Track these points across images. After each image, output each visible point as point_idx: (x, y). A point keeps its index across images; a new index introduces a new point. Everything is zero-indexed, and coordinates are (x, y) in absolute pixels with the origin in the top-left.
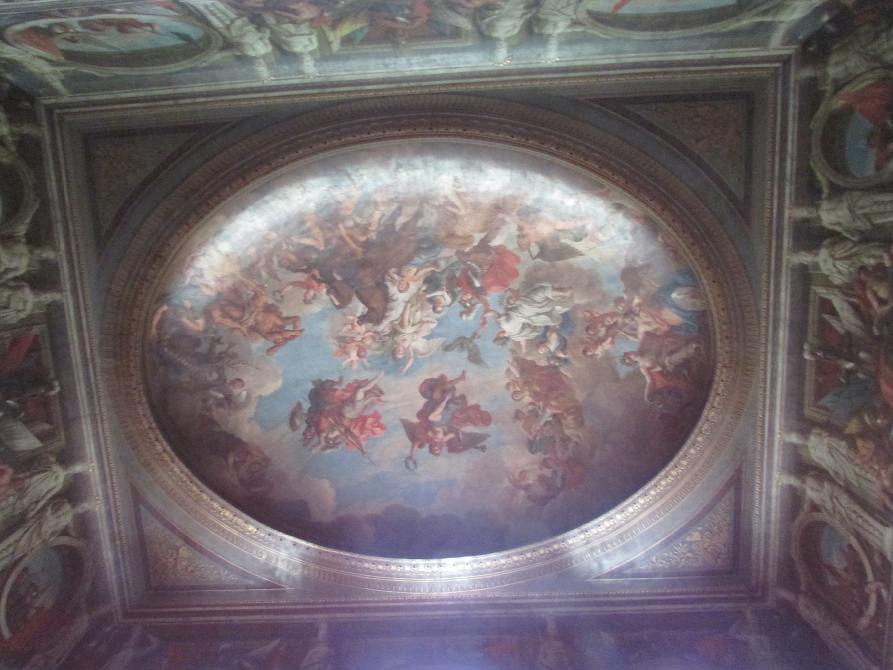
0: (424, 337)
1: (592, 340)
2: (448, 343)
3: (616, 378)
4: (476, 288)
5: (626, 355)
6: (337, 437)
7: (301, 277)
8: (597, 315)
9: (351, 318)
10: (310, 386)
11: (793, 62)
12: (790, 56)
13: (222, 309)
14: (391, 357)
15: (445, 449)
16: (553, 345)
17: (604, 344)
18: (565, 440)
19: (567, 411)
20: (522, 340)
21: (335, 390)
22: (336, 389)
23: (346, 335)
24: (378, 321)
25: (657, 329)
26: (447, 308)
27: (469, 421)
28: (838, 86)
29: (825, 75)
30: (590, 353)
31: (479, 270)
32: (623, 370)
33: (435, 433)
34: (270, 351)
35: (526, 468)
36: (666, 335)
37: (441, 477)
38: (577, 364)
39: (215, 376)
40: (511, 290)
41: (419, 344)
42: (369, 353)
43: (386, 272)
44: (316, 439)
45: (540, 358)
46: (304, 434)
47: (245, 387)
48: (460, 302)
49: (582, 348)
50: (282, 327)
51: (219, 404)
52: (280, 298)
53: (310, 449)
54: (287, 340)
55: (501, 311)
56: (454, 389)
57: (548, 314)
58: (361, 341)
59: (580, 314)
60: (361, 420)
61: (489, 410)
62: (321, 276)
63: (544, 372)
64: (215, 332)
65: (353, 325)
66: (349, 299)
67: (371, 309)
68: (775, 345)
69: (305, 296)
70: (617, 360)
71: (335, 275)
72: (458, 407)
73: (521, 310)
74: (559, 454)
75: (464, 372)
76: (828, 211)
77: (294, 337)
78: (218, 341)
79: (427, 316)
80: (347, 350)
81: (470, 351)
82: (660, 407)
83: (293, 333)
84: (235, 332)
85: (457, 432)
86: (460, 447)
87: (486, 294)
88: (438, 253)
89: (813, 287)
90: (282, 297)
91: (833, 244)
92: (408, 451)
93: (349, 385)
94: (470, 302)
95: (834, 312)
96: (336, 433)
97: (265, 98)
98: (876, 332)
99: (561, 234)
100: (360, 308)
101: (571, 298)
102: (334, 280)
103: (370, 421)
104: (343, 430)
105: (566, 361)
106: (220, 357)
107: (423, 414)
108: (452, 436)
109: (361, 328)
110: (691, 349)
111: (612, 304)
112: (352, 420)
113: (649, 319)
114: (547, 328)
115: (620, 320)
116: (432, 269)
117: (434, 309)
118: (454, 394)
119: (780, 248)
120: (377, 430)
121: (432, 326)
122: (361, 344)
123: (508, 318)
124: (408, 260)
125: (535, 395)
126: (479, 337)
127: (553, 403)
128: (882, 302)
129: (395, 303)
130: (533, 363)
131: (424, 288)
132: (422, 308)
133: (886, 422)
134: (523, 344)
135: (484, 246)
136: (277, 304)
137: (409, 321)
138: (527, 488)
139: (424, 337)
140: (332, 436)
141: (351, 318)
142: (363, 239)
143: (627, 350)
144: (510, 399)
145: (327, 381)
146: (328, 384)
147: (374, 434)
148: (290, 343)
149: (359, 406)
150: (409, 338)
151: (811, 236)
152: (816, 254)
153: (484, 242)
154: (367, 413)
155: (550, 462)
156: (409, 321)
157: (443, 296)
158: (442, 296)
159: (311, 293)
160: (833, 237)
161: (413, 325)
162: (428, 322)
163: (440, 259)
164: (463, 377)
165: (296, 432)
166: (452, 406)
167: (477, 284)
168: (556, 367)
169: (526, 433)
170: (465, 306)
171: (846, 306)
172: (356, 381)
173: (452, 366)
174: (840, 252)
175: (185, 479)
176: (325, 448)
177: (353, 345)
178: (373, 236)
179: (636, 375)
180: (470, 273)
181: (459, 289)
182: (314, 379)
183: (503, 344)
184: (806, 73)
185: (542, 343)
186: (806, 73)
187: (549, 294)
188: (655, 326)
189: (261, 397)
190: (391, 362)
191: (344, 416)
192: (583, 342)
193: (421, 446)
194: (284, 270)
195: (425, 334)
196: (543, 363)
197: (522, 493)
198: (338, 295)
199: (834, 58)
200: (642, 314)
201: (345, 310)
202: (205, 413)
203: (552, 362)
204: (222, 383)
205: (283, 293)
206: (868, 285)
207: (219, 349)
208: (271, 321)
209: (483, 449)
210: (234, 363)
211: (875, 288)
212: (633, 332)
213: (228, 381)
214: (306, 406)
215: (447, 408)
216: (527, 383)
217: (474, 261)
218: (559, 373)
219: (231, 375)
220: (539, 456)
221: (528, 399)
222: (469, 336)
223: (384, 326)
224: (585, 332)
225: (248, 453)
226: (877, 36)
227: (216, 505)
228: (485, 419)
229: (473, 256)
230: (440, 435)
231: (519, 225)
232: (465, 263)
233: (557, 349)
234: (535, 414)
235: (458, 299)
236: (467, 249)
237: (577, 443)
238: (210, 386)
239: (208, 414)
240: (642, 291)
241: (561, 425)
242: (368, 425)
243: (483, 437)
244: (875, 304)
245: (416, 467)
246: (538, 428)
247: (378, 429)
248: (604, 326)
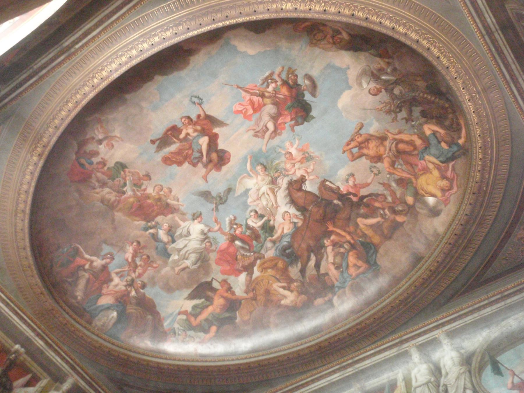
0: (250, 190)
1: (140, 252)
2: (231, 193)
3: (105, 242)
4: (237, 240)
5: (113, 259)
6: (268, 87)
7: (363, 192)
8: (150, 268)
9: (311, 177)
10: (313, 113)
13: (415, 148)
14: (265, 164)
15: (180, 125)
16: (162, 234)
17: (131, 255)
18: (104, 185)
19: (119, 201)
20: (183, 224)
21: (292, 120)
22: (292, 120)
23: (308, 163)
24: (291, 183)
25: (108, 287)
26: (247, 217)
27: (179, 152)
30: (135, 244)
31: (242, 252)
32: (106, 249)
33: (195, 130)
34: (362, 126)
35: (112, 151)
36: (100, 289)
37: (168, 104)
38: (138, 233)
39: (396, 91)
40: (213, 251)
41: (251, 183)
42: (283, 159)
43: (304, 220)
44: (284, 76)
45: (164, 221)
46: (297, 76)
47: (367, 91)
48: (242, 225)
49: (142, 243)
50: (360, 148)
51: (381, 70)
52: (373, 169)
53: (283, 68)
54: (352, 140)
55: (210, 235)
56: (205, 166)
57: (179, 250)
58: (294, 164)
59: (159, 262)
60: (257, 108)
61: (169, 167)
62: (350, 198)
63: (154, 214)
64: (413, 126)
65: (308, 173)
66: (320, 189)
67: (300, 189)
68: (38, 335)
69: (355, 179)
70: (115, 252)
71: (340, 203)
72: (193, 157)
73: (198, 242)
74: (99, 174)
75: (206, 181)
77: (348, 144)
78: (407, 120)
79: (257, 205)
80: (301, 153)
81: (213, 197)
82: (66, 249)
83: (350, 147)
84: (397, 131)
85: (181, 141)
86: (169, 133)
87: (228, 239)
88: (276, 250)
89: (48, 379)
90: (372, 171)
92: (205, 107)
93: (284, 128)
94: (234, 228)
96: (270, 89)
97: (437, 321)
99: (208, 303)
100: (308, 187)
101: (173, 268)
102: (339, 199)
103: (251, 111)
104: (267, 94)
105: (146, 229)
106: (400, 108)
107: (213, 139)
108: (182, 136)
109: (299, 174)
110: (79, 294)
111: (146, 281)
112: (264, 105)
113: (117, 289)
114: (173, 241)
115: (133, 275)
116: (274, 238)
117: (256, 212)
118: (202, 163)
119: (83, 378)
120: (240, 108)
121: (249, 200)
122: (293, 162)
123: (203, 233)
124: (294, 235)
125: (148, 197)
126: (213, 210)
127: (131, 200)
129: (285, 203)
130: (165, 215)
131: (272, 223)
132: (265, 208)
134: (181, 223)
135: (249, 269)
136: (374, 164)
137: (268, 194)
138: (100, 142)
139: (250, 190)
140: (273, 85)
141: (311, 177)
142: (333, 237)
143: (114, 261)
144: (162, 184)
145: (302, 124)
146: (300, 120)
147: (240, 104)
148: (349, 139)
149: (266, 118)
150: (261, 183)
153: (251, 273)
154: (257, 115)
155: (100, 166)
156: (268, 194)
157: (256, 224)
158: (256, 223)
159: (351, 183)
161: (264, 193)
162: (255, 201)
163: (272, 247)
164: (205, 178)
165: (303, 74)
166: (198, 155)
167: (238, 243)
168: (149, 222)
169: (132, 170)
170: (236, 224)
172: (280, 134)
173: (218, 181)
175: (374, 18)
176: (272, 74)
177: (299, 158)
178: (327, 242)
179: (96, 253)
180: (247, 247)
181: (247, 234)
182: (314, 120)
183: (194, 215)
185: (170, 230)
187: (188, 263)
188: (111, 287)
189: (350, 88)
190: (263, 160)
191: (274, 104)
192: (145, 247)
193: (199, 116)
194: (380, 193)
195: (250, 193)
196: (159, 219)
197: (101, 136)
198: (331, 190)
200: (124, 288)
201: (319, 181)
202: (390, 61)
203: (153, 223)
204: (388, 87)
205: (373, 174)
207: (404, 114)
208: (372, 149)
209: (153, 142)
210: (386, 106)
212: (121, 275)
213: (383, 90)
214: (308, 97)
215: (200, 152)
216: (159, 200)
217: (250, 256)
218: (145, 219)
219: (384, 96)
220: (111, 164)
221: (150, 191)
222: (220, 207)
223: (283, 182)
224: (148, 254)
225: (334, 43)
227: (333, 9)
228: (167, 161)
229: (252, 259)
230: (190, 131)
231: (235, 295)
232: (255, 253)
233: (157, 233)
234: (137, 185)
235: (244, 227)
236: (258, 262)
237: (94, 188)
238: (396, 83)
239: (387, 60)
240: (134, 301)
241: (114, 191)
242: (249, 108)
243: (160, 148)
245: (191, 100)
246: (128, 178)
247: (240, 109)
248: (140, 266)
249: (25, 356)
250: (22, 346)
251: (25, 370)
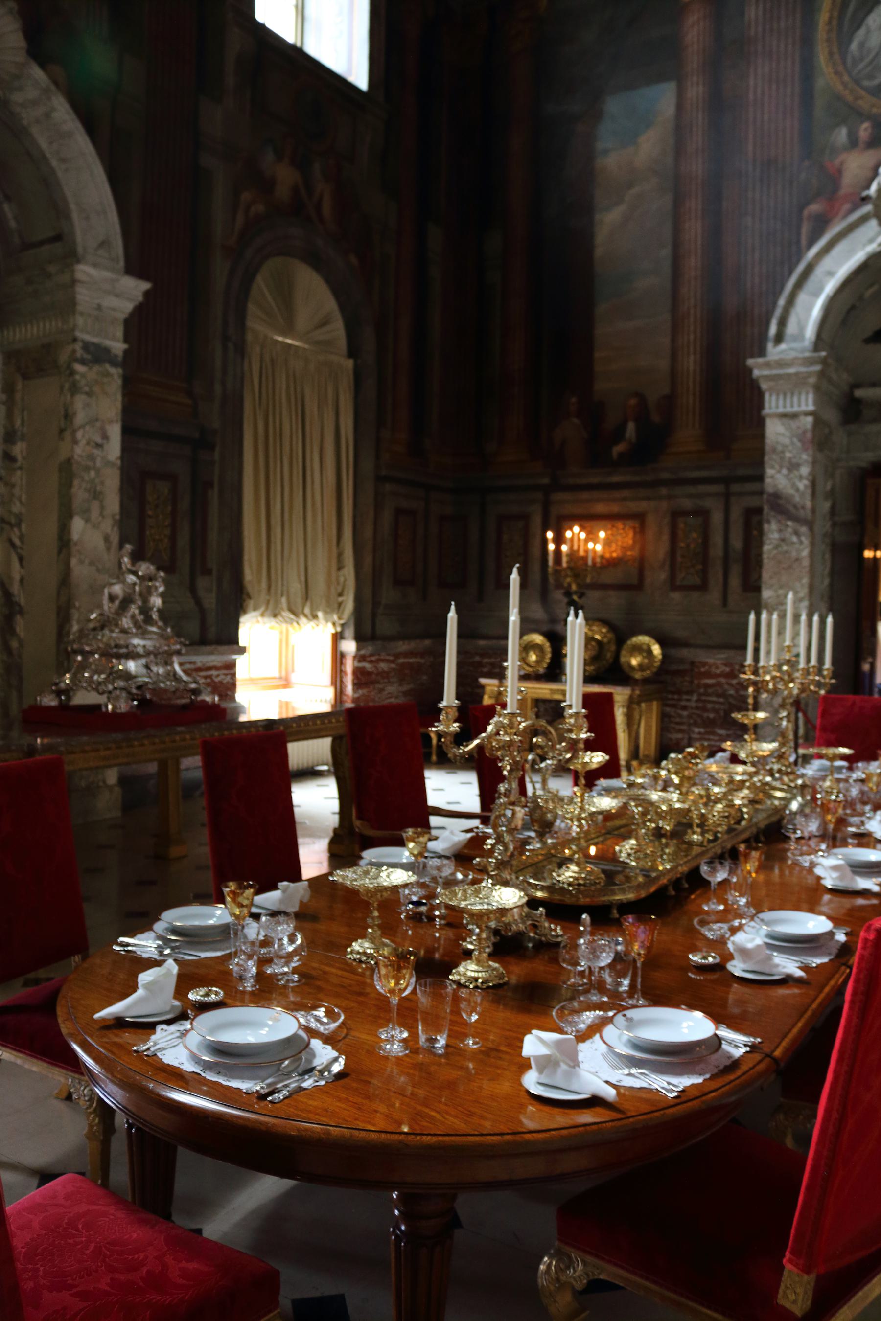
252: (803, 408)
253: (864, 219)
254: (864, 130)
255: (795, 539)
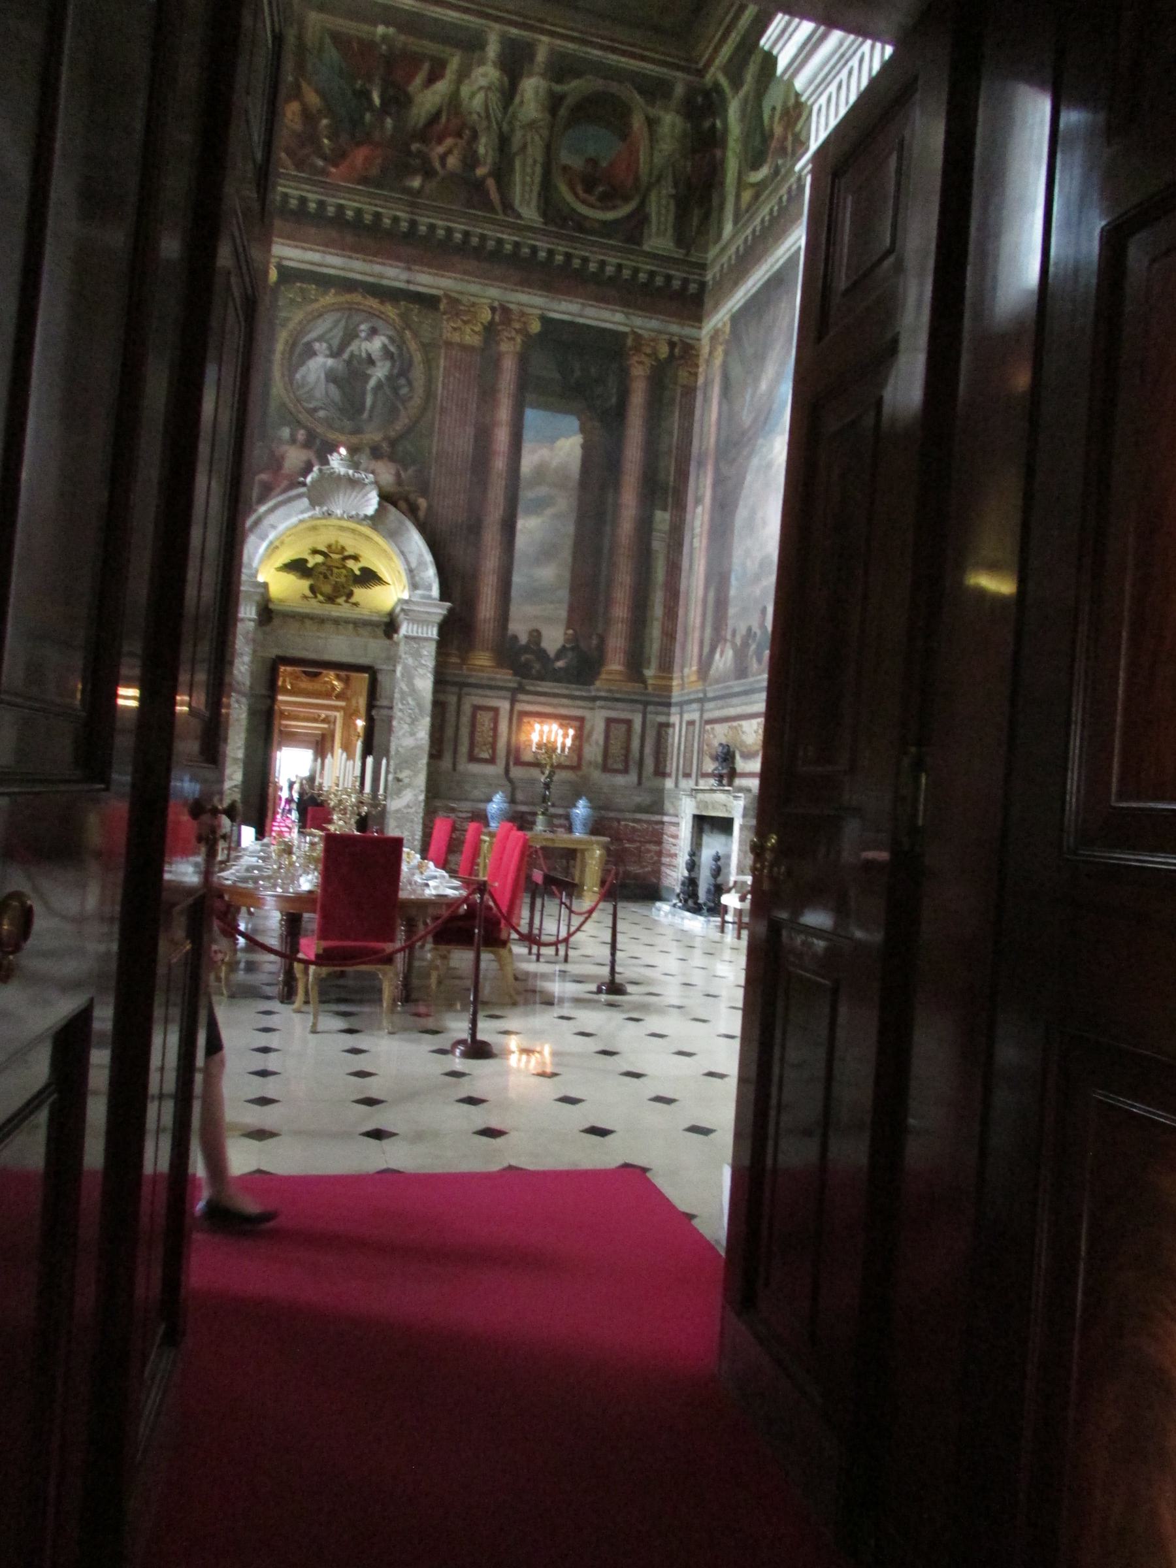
11: (697, 79)
12: (703, 77)
28: (652, 123)
29: (666, 109)
76: (537, 87)
91: (503, 92)
95: (432, 79)
98: (415, 147)
119: (511, 23)
128: (443, 158)
133: (328, 151)
151: (514, 63)
152: (495, 64)
160: (509, 93)
171: (437, 99)
174: (494, 97)
184: (679, 90)
186: (679, 90)
199: (679, 120)
206: (460, 141)
211: (456, 152)
226: (676, 185)
244: (441, 149)
249: (402, 37)
250: (387, 24)
251: (413, 60)
252: (248, 616)
253: (300, 496)
254: (301, 435)
255: (236, 705)
